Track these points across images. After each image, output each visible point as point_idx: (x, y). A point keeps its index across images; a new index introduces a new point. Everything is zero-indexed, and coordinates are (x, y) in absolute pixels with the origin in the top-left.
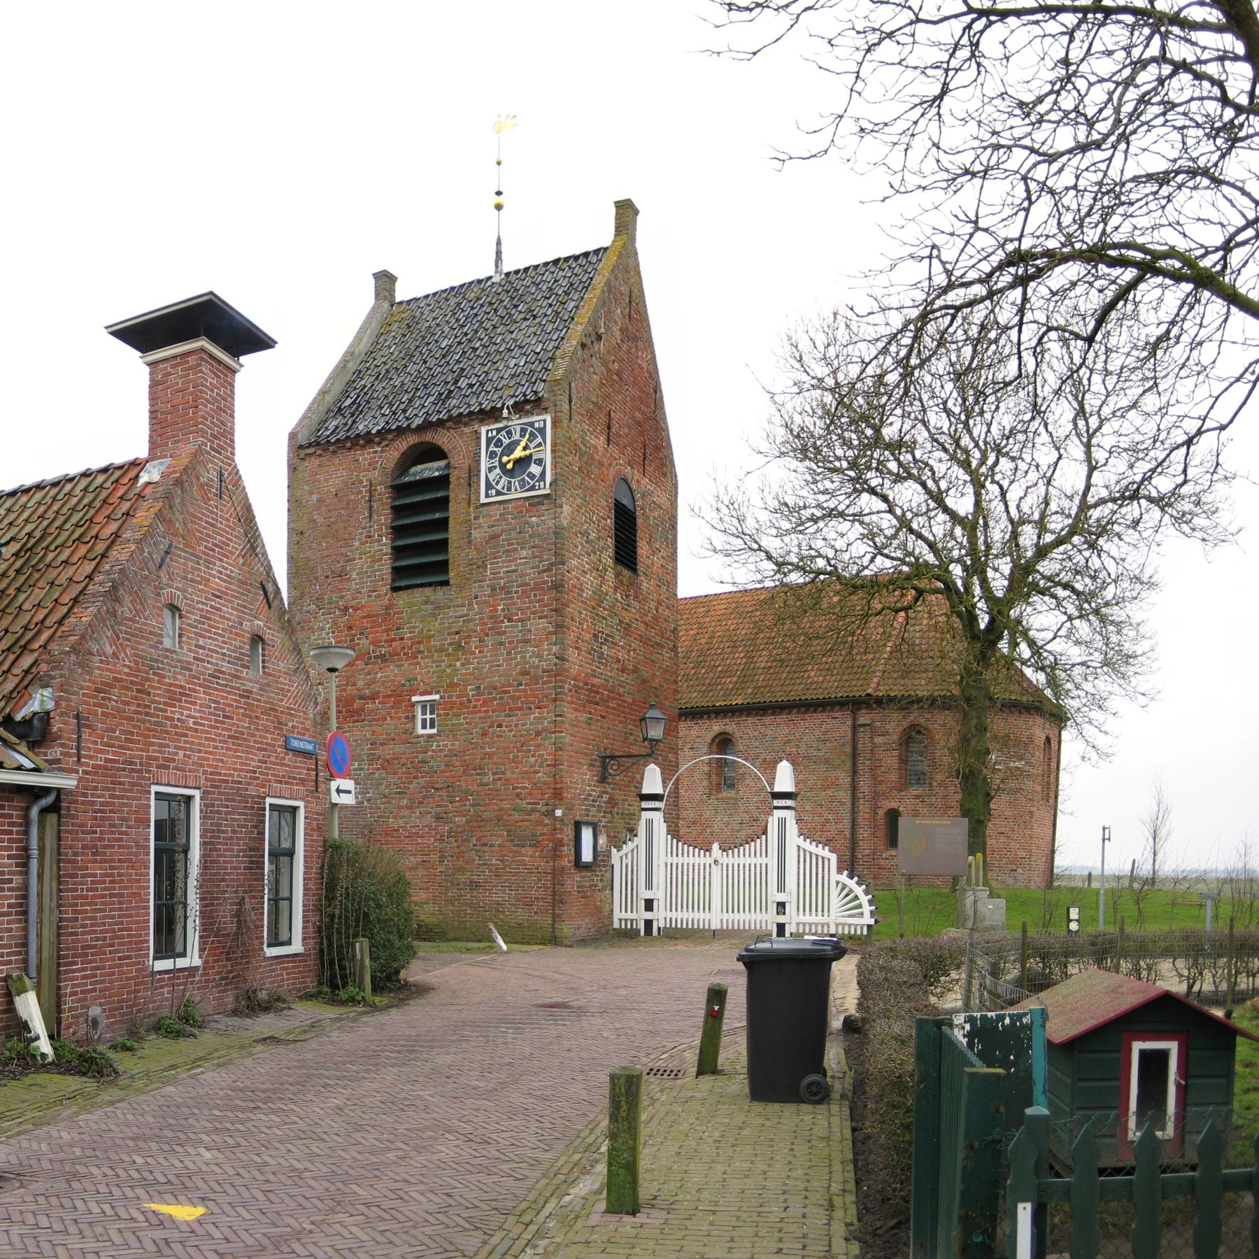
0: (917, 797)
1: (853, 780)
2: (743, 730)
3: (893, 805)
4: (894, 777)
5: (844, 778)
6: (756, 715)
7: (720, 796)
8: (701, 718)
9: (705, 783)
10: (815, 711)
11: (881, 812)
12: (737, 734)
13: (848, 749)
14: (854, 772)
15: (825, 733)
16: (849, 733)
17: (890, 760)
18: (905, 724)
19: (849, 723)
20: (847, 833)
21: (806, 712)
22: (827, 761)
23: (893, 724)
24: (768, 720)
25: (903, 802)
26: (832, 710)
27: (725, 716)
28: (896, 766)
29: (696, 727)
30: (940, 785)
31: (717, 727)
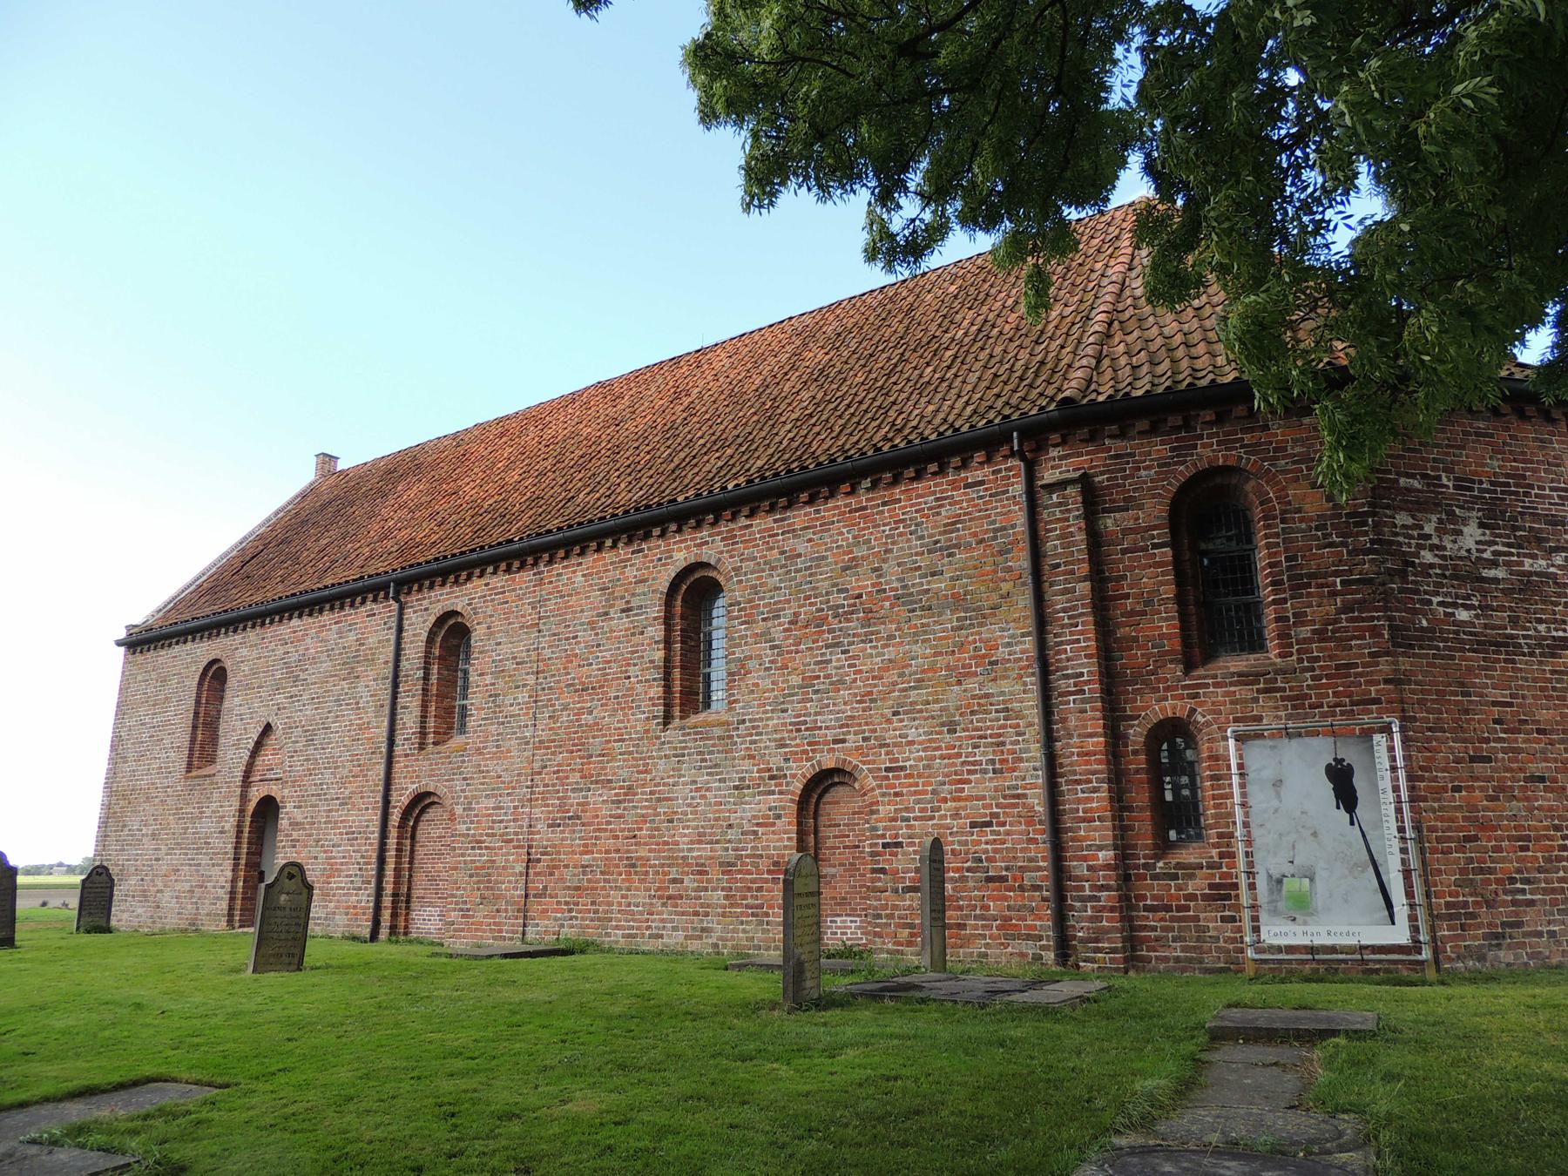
0: (1245, 678)
1: (1042, 645)
2: (736, 551)
3: (1171, 707)
4: (1165, 624)
5: (1012, 637)
6: (772, 509)
7: (693, 719)
8: (647, 537)
9: (657, 691)
10: (918, 477)
11: (1136, 734)
12: (728, 564)
13: (1021, 561)
14: (1042, 622)
15: (950, 527)
16: (1020, 520)
17: (1150, 579)
18: (1184, 471)
19: (1018, 488)
20: (1039, 805)
21: (896, 481)
22: (958, 601)
23: (1150, 472)
24: (800, 517)
25: (1212, 698)
26: (964, 465)
27: (699, 526)
28: (1168, 591)
29: (638, 560)
30: (1321, 635)
31: (680, 551)
